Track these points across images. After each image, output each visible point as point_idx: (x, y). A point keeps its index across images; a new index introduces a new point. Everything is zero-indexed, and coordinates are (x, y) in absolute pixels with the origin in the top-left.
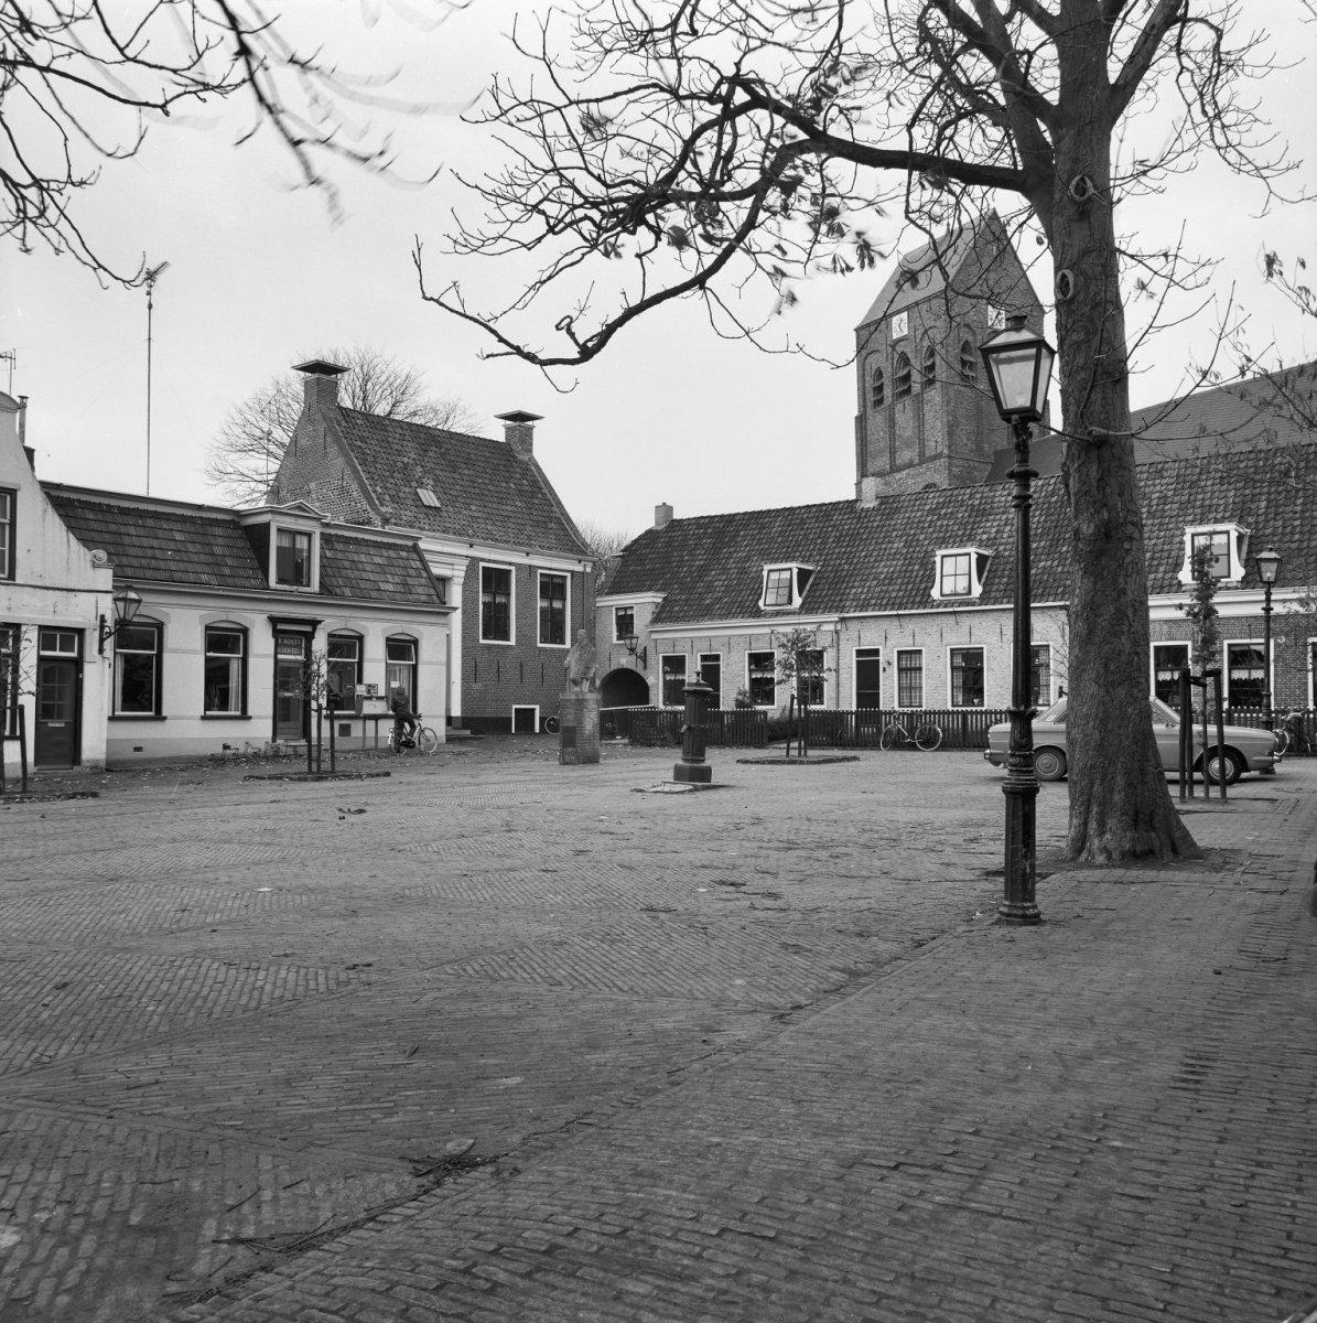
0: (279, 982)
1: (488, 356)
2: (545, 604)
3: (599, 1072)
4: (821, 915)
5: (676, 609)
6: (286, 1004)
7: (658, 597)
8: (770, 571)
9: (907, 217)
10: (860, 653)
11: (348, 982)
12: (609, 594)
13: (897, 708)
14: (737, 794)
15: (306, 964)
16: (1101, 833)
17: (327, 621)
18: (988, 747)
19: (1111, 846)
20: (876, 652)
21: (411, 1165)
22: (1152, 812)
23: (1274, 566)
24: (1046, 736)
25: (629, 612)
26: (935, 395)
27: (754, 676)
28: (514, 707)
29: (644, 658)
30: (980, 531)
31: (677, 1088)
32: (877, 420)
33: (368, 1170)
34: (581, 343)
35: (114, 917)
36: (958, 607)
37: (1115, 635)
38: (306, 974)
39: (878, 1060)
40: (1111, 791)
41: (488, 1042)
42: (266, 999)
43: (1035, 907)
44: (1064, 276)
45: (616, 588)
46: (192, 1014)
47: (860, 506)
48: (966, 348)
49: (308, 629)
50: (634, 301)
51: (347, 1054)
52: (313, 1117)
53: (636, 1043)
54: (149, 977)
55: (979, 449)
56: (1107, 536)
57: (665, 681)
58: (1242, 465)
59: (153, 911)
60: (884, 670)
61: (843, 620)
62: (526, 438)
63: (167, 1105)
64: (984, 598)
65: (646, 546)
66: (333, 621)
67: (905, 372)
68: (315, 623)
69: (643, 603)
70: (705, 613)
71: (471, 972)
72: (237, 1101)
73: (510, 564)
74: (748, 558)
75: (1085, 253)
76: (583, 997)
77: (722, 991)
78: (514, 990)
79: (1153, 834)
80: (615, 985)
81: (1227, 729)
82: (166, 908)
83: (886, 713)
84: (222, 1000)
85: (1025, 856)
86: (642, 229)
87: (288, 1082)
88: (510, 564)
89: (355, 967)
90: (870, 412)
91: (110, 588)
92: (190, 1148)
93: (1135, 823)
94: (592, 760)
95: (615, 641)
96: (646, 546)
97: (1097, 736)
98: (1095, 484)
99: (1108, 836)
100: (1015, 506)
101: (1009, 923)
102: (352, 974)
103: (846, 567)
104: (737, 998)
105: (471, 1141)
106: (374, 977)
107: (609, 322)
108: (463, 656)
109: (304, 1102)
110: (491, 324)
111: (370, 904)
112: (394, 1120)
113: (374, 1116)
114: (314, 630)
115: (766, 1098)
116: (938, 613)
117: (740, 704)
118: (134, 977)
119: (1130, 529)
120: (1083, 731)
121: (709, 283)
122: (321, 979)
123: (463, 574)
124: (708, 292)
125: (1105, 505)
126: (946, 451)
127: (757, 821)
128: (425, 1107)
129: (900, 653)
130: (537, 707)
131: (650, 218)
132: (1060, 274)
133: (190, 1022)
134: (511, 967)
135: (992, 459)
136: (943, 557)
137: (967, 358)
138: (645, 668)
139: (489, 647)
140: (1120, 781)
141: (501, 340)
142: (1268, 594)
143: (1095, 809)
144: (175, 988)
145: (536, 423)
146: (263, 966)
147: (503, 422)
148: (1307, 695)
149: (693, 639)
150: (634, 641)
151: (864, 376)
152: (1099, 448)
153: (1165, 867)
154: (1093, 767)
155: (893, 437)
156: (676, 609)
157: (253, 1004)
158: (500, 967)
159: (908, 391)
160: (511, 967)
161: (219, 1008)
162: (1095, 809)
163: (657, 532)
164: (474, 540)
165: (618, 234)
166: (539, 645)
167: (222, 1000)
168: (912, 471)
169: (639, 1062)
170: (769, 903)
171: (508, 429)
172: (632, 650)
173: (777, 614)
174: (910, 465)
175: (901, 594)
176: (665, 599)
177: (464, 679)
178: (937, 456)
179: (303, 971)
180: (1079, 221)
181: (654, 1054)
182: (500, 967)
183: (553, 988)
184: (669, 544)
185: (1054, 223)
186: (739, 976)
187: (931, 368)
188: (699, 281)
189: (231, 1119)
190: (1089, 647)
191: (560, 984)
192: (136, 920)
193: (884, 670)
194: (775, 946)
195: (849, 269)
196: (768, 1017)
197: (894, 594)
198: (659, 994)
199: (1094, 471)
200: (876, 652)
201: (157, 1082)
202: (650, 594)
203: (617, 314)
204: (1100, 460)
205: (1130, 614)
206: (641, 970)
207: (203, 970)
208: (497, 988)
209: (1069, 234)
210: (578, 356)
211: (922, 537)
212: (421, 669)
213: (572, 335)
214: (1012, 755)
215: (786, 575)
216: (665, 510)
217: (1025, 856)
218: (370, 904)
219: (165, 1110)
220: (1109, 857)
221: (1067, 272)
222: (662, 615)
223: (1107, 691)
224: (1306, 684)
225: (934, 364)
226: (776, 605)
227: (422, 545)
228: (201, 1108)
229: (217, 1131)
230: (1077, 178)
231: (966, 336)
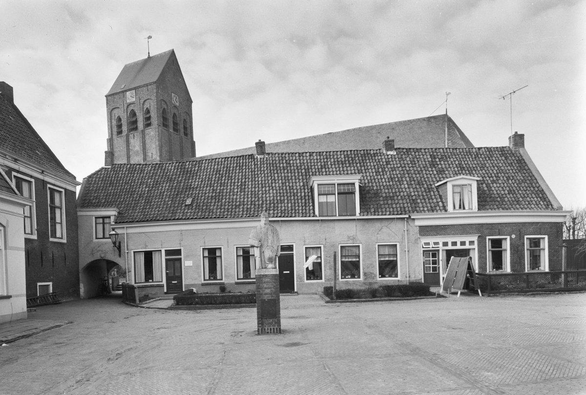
13: (133, 283)
48: (164, 111)
159: (136, 129)
225: (150, 117)
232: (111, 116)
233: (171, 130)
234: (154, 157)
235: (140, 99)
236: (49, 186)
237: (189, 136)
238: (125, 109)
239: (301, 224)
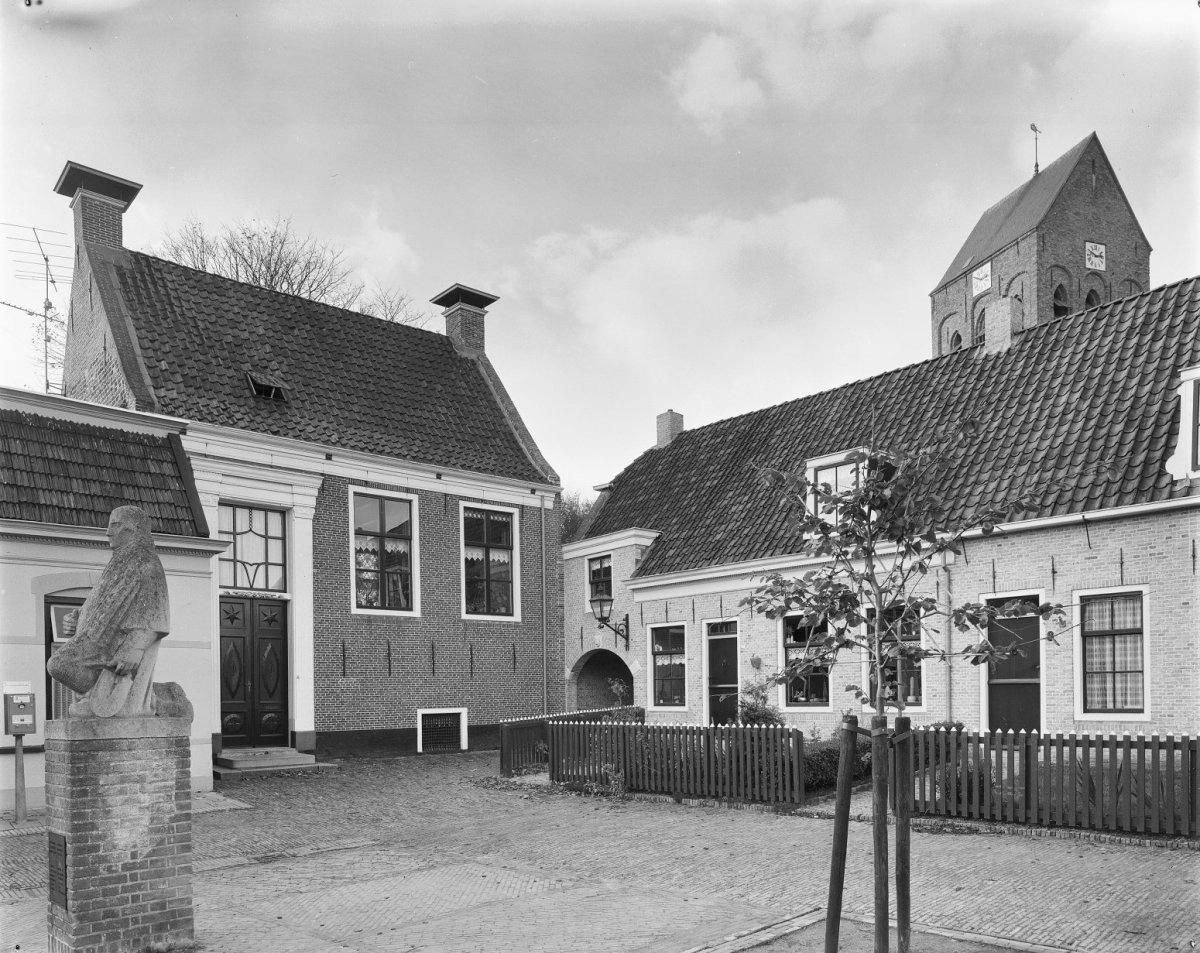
2: (477, 554)
5: (671, 552)
7: (646, 538)
8: (817, 470)
25: (606, 565)
28: (421, 712)
29: (624, 633)
48: (1059, 293)
57: (657, 669)
62: (474, 330)
65: (642, 472)
69: (625, 546)
73: (408, 490)
123: (313, 502)
129: (1086, 601)
130: (464, 712)
137: (1061, 304)
138: (627, 647)
139: (370, 619)
151: (940, 343)
156: (671, 552)
163: (660, 451)
164: (332, 450)
166: (465, 616)
177: (319, 674)
184: (673, 464)
202: (632, 532)
216: (675, 418)
222: (652, 564)
227: (189, 443)
231: (1060, 279)
232: (940, 337)
235: (1000, 280)
238: (969, 311)
239: (1024, 539)
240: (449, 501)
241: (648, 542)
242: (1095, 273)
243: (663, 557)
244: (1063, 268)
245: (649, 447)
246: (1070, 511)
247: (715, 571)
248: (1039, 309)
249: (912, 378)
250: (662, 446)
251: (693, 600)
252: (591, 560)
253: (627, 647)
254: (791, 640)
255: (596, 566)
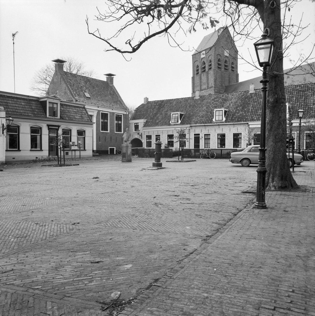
0: (52, 230)
1: (107, 51)
3: (155, 262)
4: (203, 205)
5: (149, 123)
6: (54, 237)
7: (145, 121)
8: (173, 114)
9: (224, 12)
10: (195, 135)
11: (73, 229)
12: (133, 120)
14: (169, 170)
15: (60, 223)
16: (273, 182)
17: (62, 126)
18: (231, 158)
19: (276, 185)
20: (199, 134)
21: (100, 305)
22: (286, 176)
23: (302, 113)
24: (245, 155)
25: (138, 124)
26: (211, 72)
27: (169, 140)
28: (109, 148)
29: (141, 136)
30: (225, 105)
31: (183, 270)
32: (197, 78)
33: (85, 308)
34: (133, 47)
35: (3, 208)
36: (219, 124)
37: (278, 129)
38: (60, 226)
39: (243, 258)
40: (276, 171)
41: (118, 250)
42: (48, 236)
43: (265, 204)
44: (267, 30)
45: (134, 118)
46: (25, 242)
47: (195, 98)
48: (219, 60)
49: (57, 128)
50: (147, 36)
51: (75, 257)
52: (65, 283)
53: (164, 250)
54: (12, 229)
55: (222, 85)
56: (277, 102)
57: (147, 142)
58: (290, 89)
59: (15, 205)
60: (201, 139)
61: (191, 126)
62: (112, 80)
63: (15, 280)
64: (226, 121)
66: (63, 126)
67: (204, 66)
68: (59, 126)
69: (141, 122)
70: (157, 124)
71: (109, 225)
72: (39, 277)
73: (108, 112)
74: (167, 111)
75: (273, 23)
76: (144, 233)
77: (184, 231)
78: (122, 231)
79: (287, 182)
80: (152, 229)
81: (295, 154)
82: (19, 205)
83: (201, 149)
84: (35, 236)
85: (263, 190)
86: (149, 16)
87: (56, 269)
88: (108, 112)
89: (74, 224)
90: (195, 76)
91: (5, 117)
92: (22, 299)
93: (282, 179)
94: (130, 161)
95: (134, 131)
96: (142, 108)
97: (272, 156)
98: (274, 88)
99: (275, 182)
100: (262, 91)
101: (258, 208)
102: (74, 226)
103: (192, 113)
104: (189, 233)
105: (119, 293)
106: (80, 227)
107: (141, 41)
108: (96, 135)
109: (62, 277)
110: (107, 41)
111: (76, 203)
112: (92, 284)
113: (86, 282)
114: (59, 128)
115: (214, 275)
116: (223, 125)
117: (166, 147)
118: (8, 228)
119: (283, 100)
120: (268, 154)
121: (168, 31)
122: (65, 228)
124: (168, 33)
125: (276, 93)
126: (214, 86)
127: (177, 177)
128: (102, 278)
129: (205, 135)
130: (115, 148)
131: (151, 12)
132: (265, 29)
133: (24, 245)
134: (120, 223)
135: (225, 88)
136: (216, 111)
137: (219, 63)
138: (142, 138)
139: (103, 133)
140: (278, 168)
141: (111, 45)
142: (300, 120)
143: (271, 175)
144: (20, 232)
145: (114, 76)
146: (47, 224)
147: (106, 76)
148: (304, 145)
149: (153, 131)
150: (139, 131)
151: (194, 67)
152: (275, 78)
153: (290, 191)
154: (271, 164)
155: (201, 82)
156: (149, 123)
157: (44, 238)
158: (117, 223)
159: (205, 71)
160: (120, 223)
161: (33, 240)
162: (271, 175)
165: (143, 16)
166: (115, 132)
167: (35, 236)
168: (205, 91)
169: (166, 258)
170: (188, 202)
171: (107, 78)
172: (138, 134)
173: (175, 125)
174: (205, 89)
175: (205, 120)
176: (146, 121)
178: (211, 87)
179: (59, 226)
180: (271, 14)
181: (170, 255)
182: (117, 223)
183: (134, 230)
185: (264, 15)
186: (187, 226)
187: (211, 65)
188: (166, 30)
189: (37, 285)
190: (271, 132)
191: (136, 229)
192: (10, 208)
193: (201, 139)
194: (194, 216)
195: (208, 28)
196: (200, 240)
197: (204, 120)
198: (166, 232)
199: (274, 84)
200: (199, 134)
201: (13, 270)
203: (143, 39)
204: (275, 81)
205: (282, 123)
206: (159, 224)
207: (29, 225)
208: (118, 231)
209: (269, 18)
210: (132, 51)
211: (211, 106)
212: (86, 138)
213: (130, 45)
214: (260, 162)
215: (177, 115)
216: (147, 99)
217: (263, 190)
218: (76, 203)
219: (14, 282)
220: (275, 188)
221: (267, 28)
222: (146, 125)
223: (276, 144)
224: (304, 143)
226: (174, 123)
227: (86, 107)
228: (28, 281)
229: (32, 291)
230: (271, 2)
231: (219, 57)
232: (194, 65)
233: (223, 70)
234: (212, 85)
236: (115, 114)
237: (235, 71)
240: (113, 113)
241: (145, 121)
242: (226, 56)
243: (148, 124)
244: (220, 55)
245: (142, 103)
246: (203, 124)
247: (157, 127)
248: (215, 64)
249: (186, 100)
250: (145, 103)
251: (153, 131)
252: (135, 123)
253: (142, 138)
254: (168, 138)
255: (136, 124)
